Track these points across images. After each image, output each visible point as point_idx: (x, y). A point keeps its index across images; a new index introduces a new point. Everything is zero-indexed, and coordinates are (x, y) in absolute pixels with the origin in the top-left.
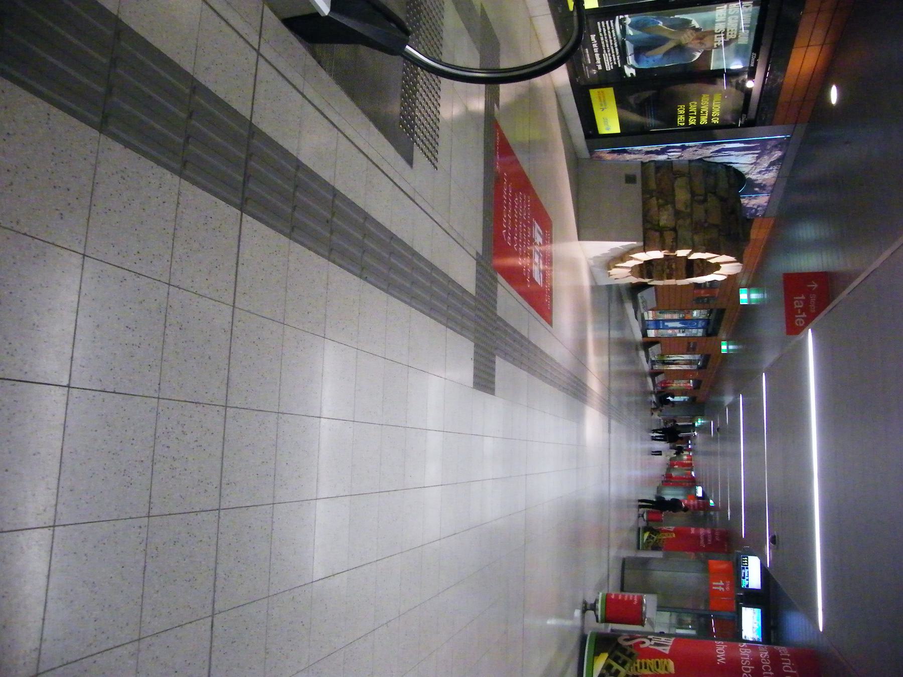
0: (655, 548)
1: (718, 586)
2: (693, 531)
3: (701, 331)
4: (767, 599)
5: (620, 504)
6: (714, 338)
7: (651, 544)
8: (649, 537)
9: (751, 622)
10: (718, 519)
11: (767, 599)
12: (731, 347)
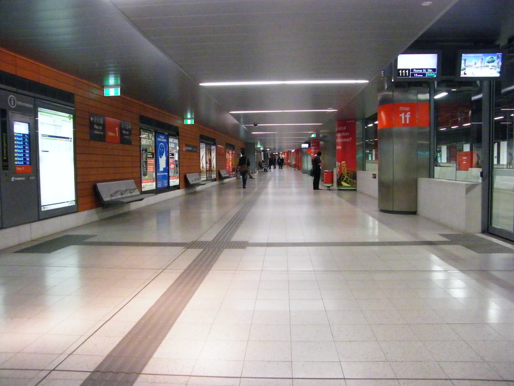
0: (354, 177)
1: (405, 118)
2: (339, 147)
3: (171, 140)
4: (449, 46)
5: (317, 203)
6: (180, 130)
7: (351, 180)
8: (345, 182)
9: (479, 66)
10: (326, 131)
11: (449, 46)
12: (189, 116)
